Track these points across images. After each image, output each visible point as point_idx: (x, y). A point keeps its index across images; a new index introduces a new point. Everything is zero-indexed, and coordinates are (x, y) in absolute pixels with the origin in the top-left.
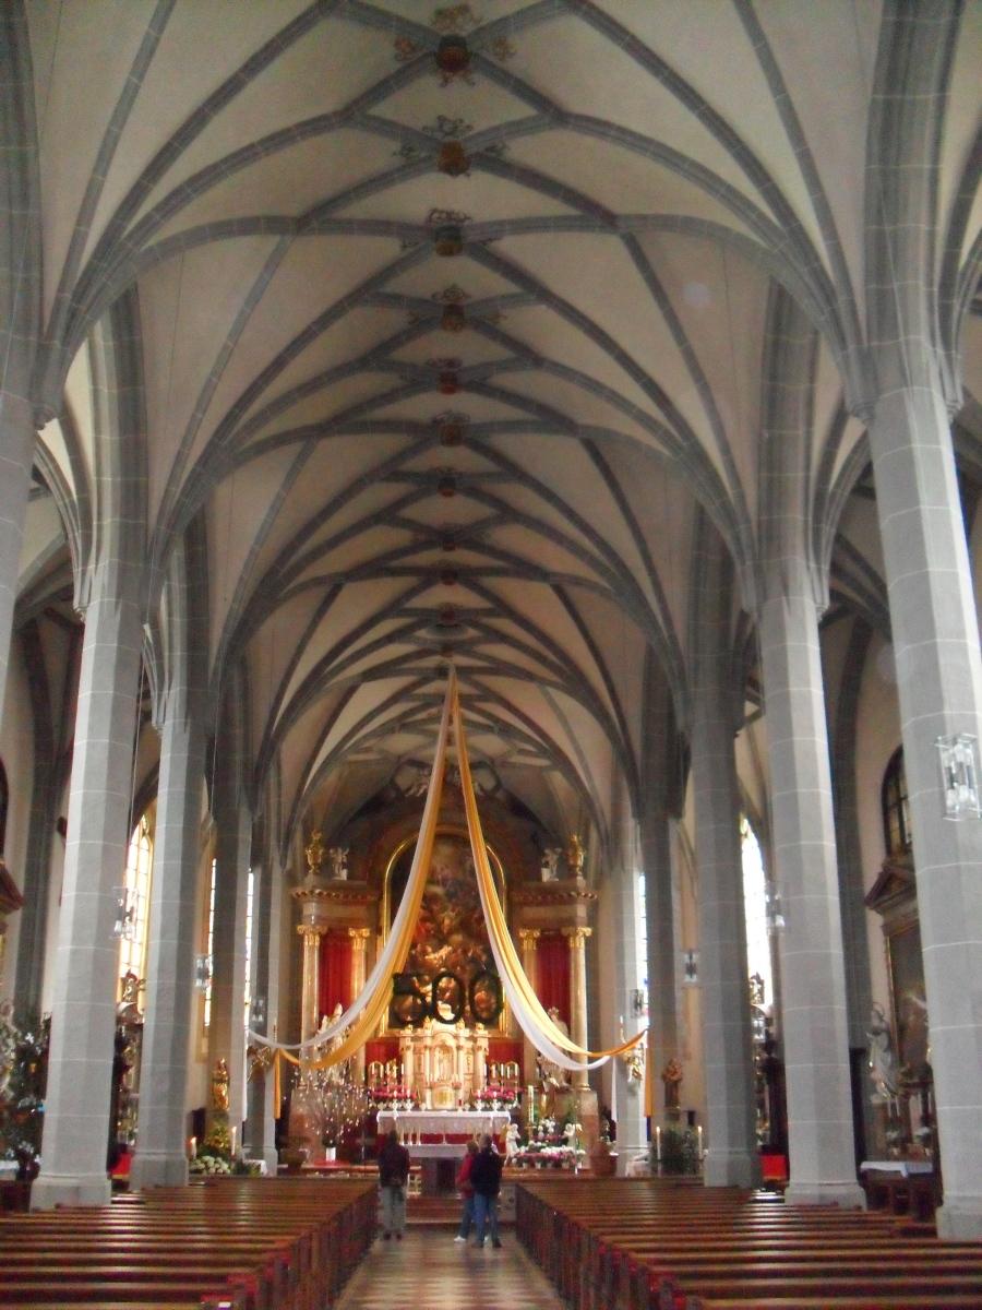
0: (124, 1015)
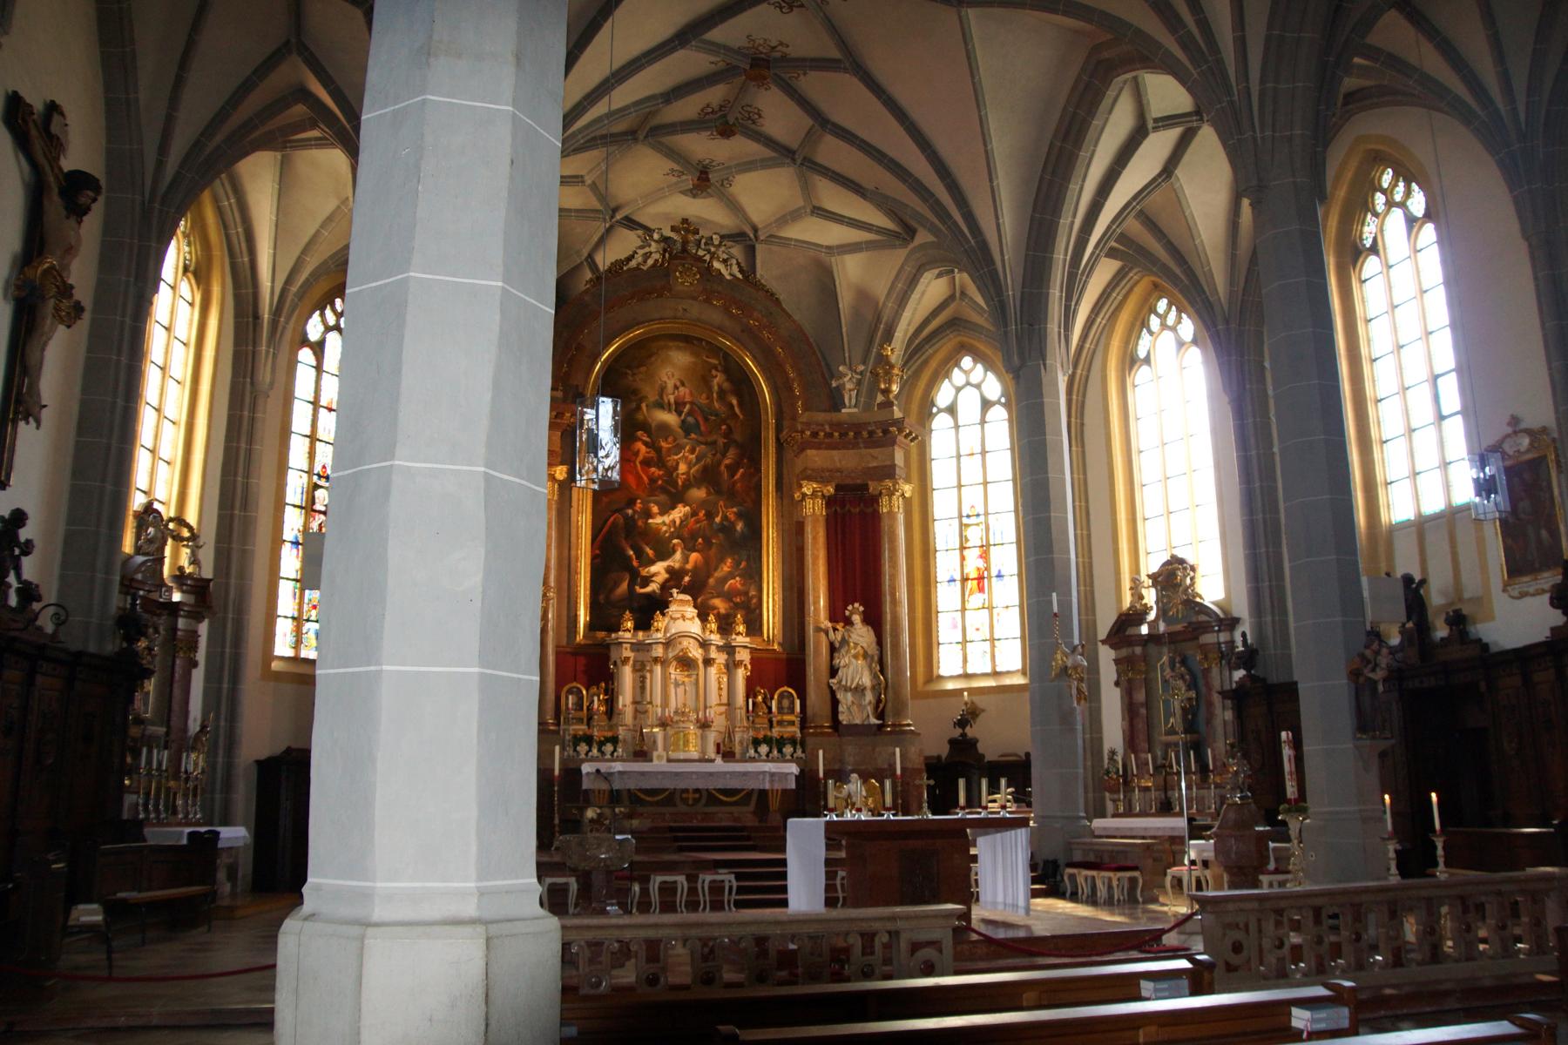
0: (139, 576)
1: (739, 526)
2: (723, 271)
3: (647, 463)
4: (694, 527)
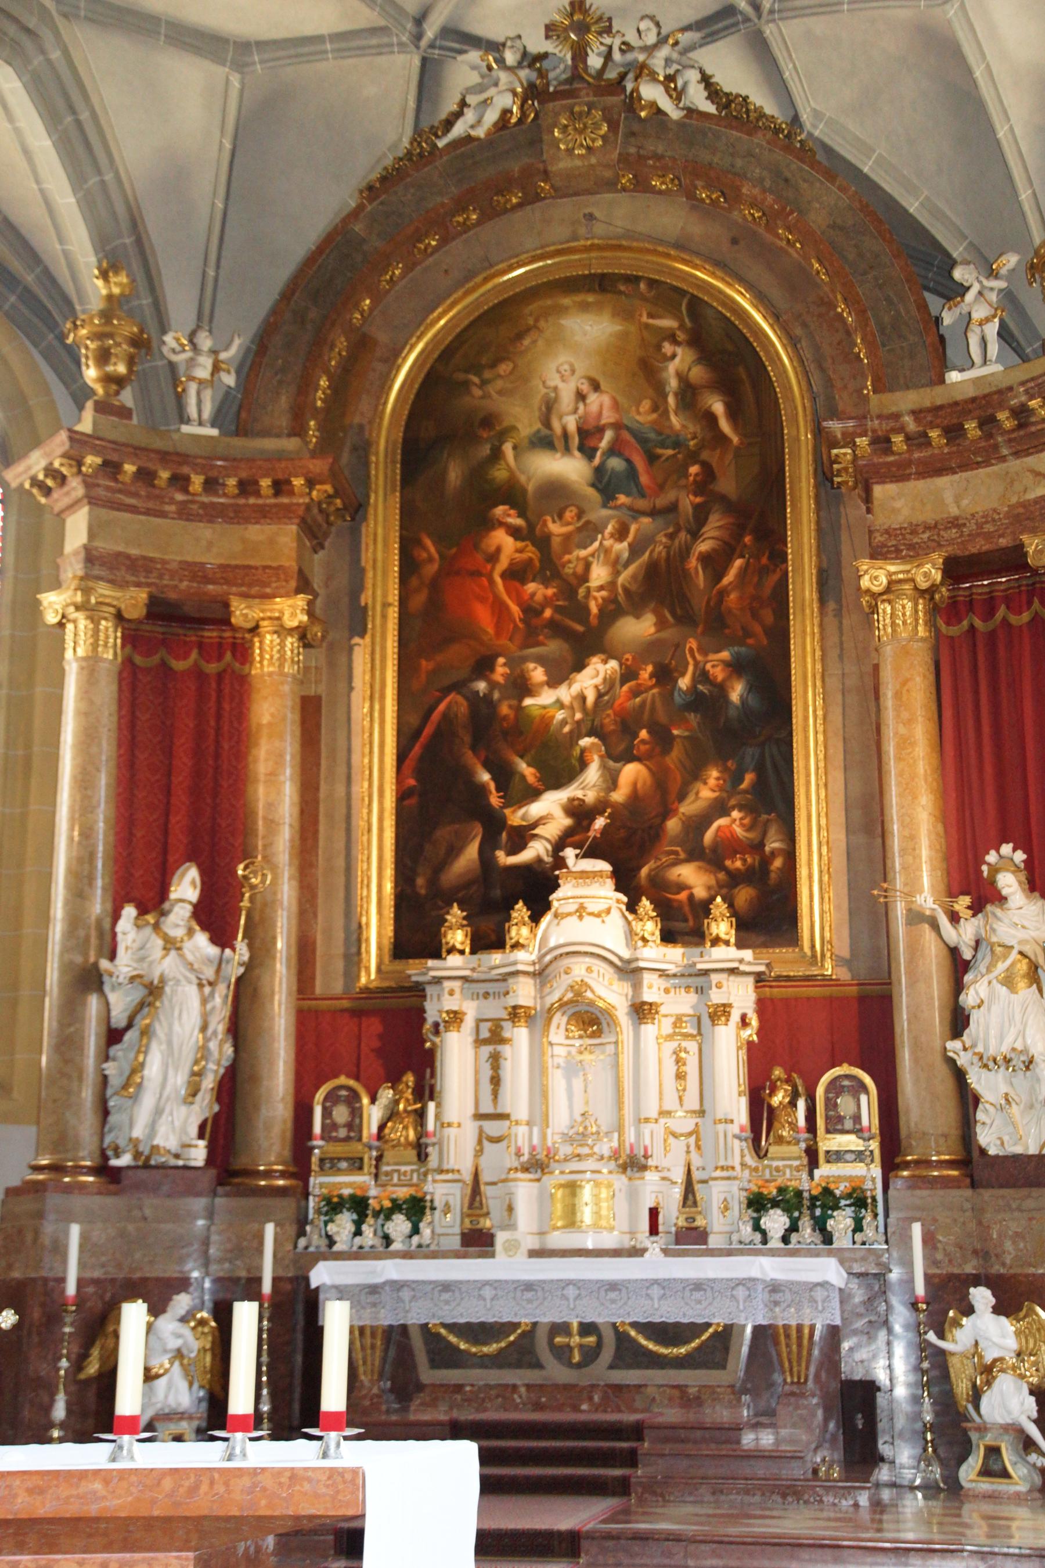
1: (737, 692)
2: (666, 104)
3: (517, 574)
4: (630, 704)
